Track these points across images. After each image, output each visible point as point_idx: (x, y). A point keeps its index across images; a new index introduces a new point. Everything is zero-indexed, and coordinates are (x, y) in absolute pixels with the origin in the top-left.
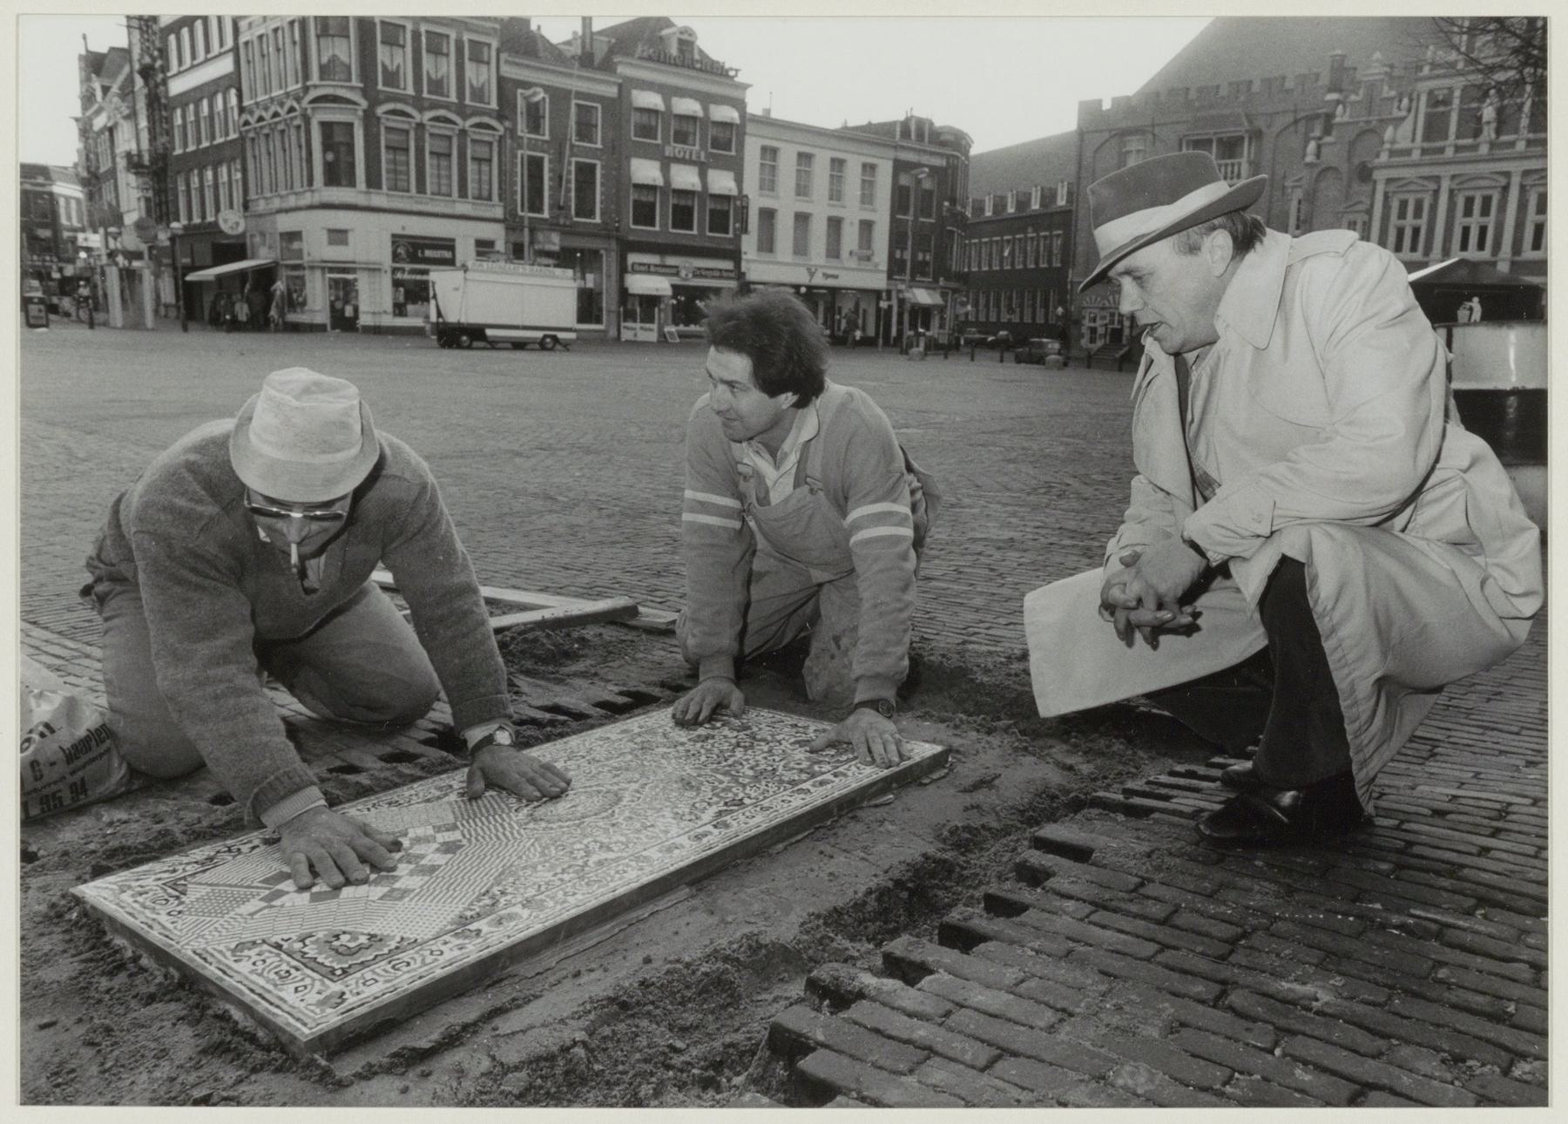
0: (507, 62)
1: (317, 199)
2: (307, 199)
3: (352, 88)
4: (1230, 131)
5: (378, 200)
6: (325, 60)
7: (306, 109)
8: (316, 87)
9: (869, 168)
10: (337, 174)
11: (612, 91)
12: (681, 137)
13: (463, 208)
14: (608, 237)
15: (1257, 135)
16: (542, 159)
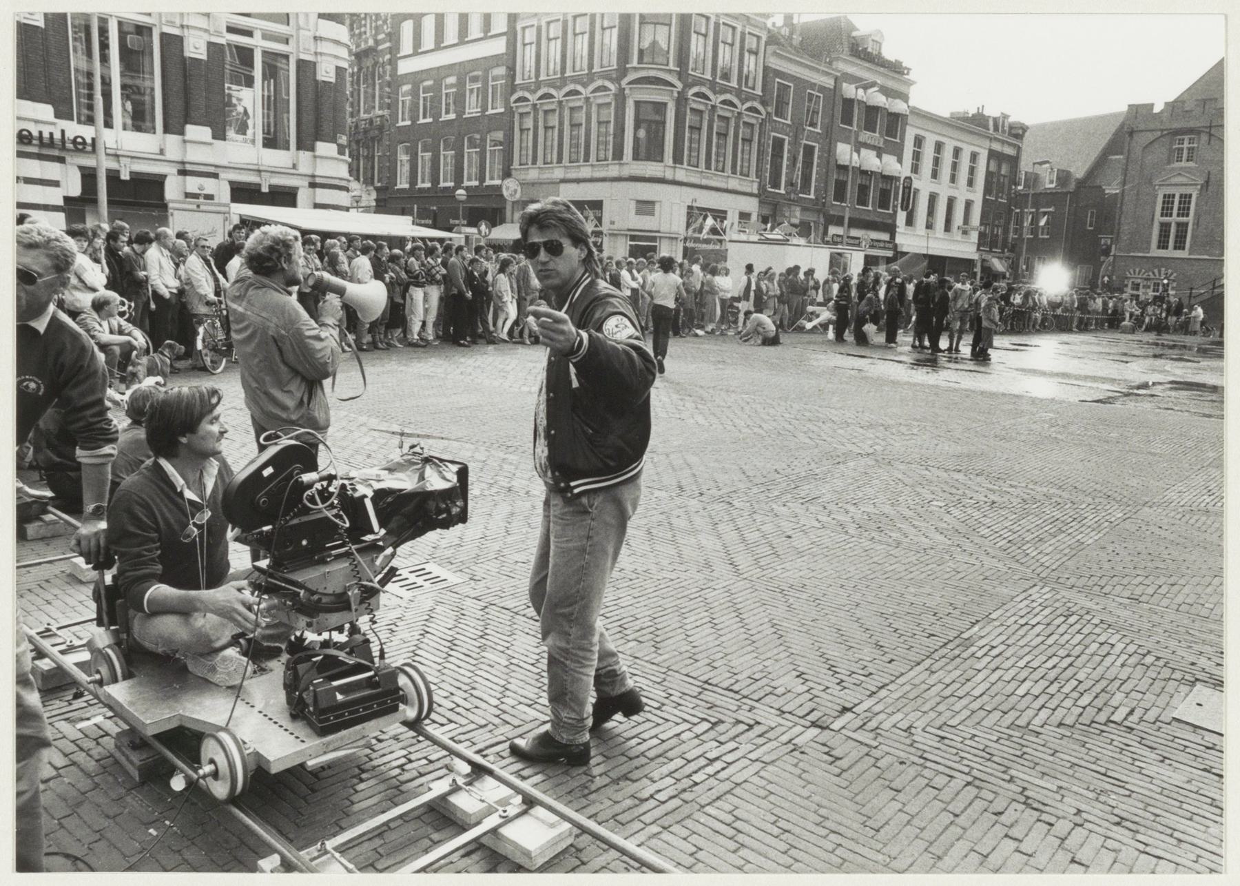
0: (775, 54)
1: (626, 172)
2: (614, 171)
3: (670, 71)
5: (681, 175)
6: (646, 44)
7: (624, 89)
8: (635, 69)
9: (974, 157)
10: (650, 150)
11: (829, 83)
12: (870, 126)
13: (733, 184)
14: (819, 211)
16: (784, 140)
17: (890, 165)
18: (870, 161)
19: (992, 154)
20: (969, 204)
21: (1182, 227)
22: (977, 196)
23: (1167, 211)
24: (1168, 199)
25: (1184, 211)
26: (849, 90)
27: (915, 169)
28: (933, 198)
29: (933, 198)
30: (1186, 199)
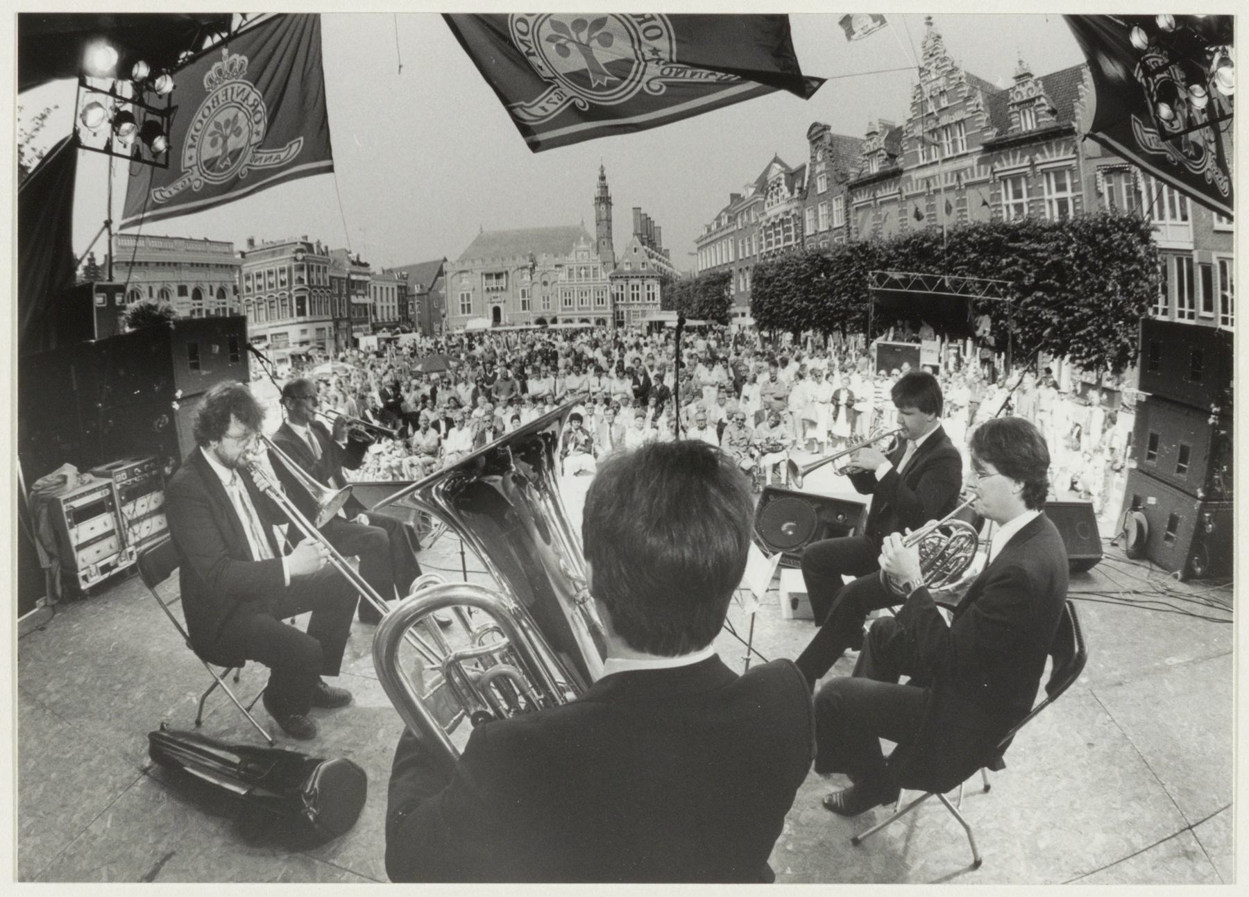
4: (499, 271)
9: (393, 289)
15: (507, 273)
17: (368, 300)
18: (361, 300)
19: (399, 287)
20: (394, 307)
21: (469, 305)
22: (396, 304)
23: (463, 300)
24: (463, 295)
25: (468, 299)
26: (354, 277)
27: (375, 300)
28: (382, 307)
29: (382, 307)
30: (468, 296)
